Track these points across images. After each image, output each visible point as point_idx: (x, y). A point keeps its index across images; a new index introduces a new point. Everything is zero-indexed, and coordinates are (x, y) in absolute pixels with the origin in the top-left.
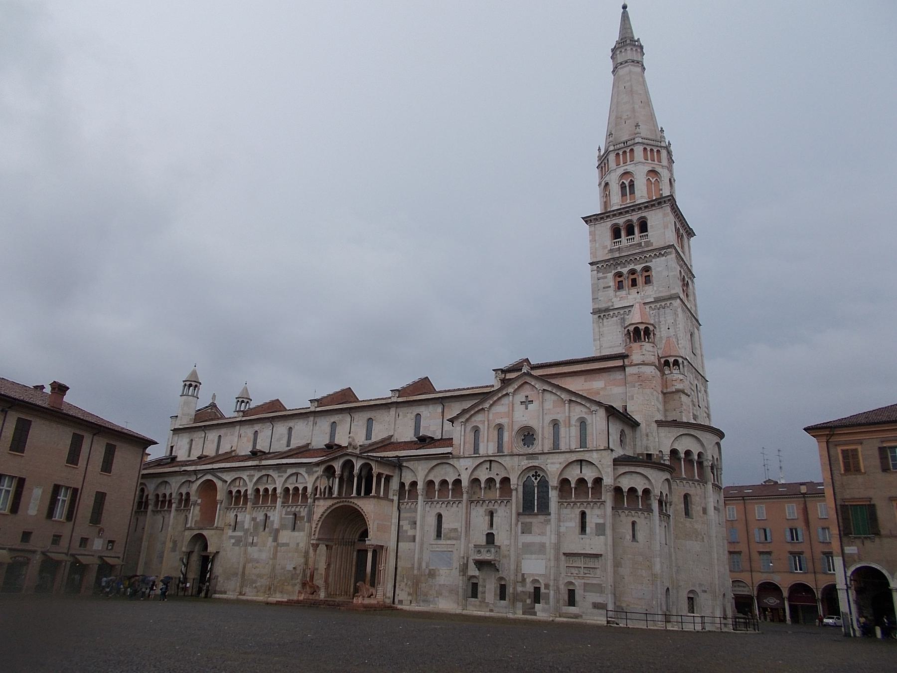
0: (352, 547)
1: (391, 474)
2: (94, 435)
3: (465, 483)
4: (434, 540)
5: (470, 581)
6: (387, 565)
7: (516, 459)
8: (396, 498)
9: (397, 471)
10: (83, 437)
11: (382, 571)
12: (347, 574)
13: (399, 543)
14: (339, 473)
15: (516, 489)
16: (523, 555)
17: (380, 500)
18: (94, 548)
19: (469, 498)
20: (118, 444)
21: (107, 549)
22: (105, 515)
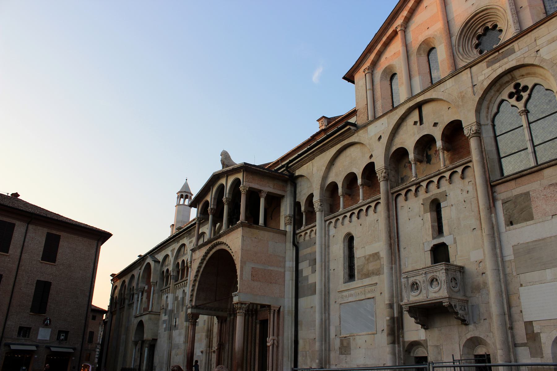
0: (254, 317)
1: (279, 192)
2: (28, 224)
3: (380, 165)
4: (345, 283)
5: (412, 354)
6: (280, 337)
7: (465, 76)
8: (289, 229)
9: (289, 188)
10: (14, 225)
11: (271, 348)
12: (249, 357)
13: (301, 301)
14: (212, 207)
15: (478, 134)
16: (522, 276)
17: (256, 231)
18: (39, 337)
19: (392, 188)
20: (62, 234)
21: (58, 338)
22: (51, 304)
